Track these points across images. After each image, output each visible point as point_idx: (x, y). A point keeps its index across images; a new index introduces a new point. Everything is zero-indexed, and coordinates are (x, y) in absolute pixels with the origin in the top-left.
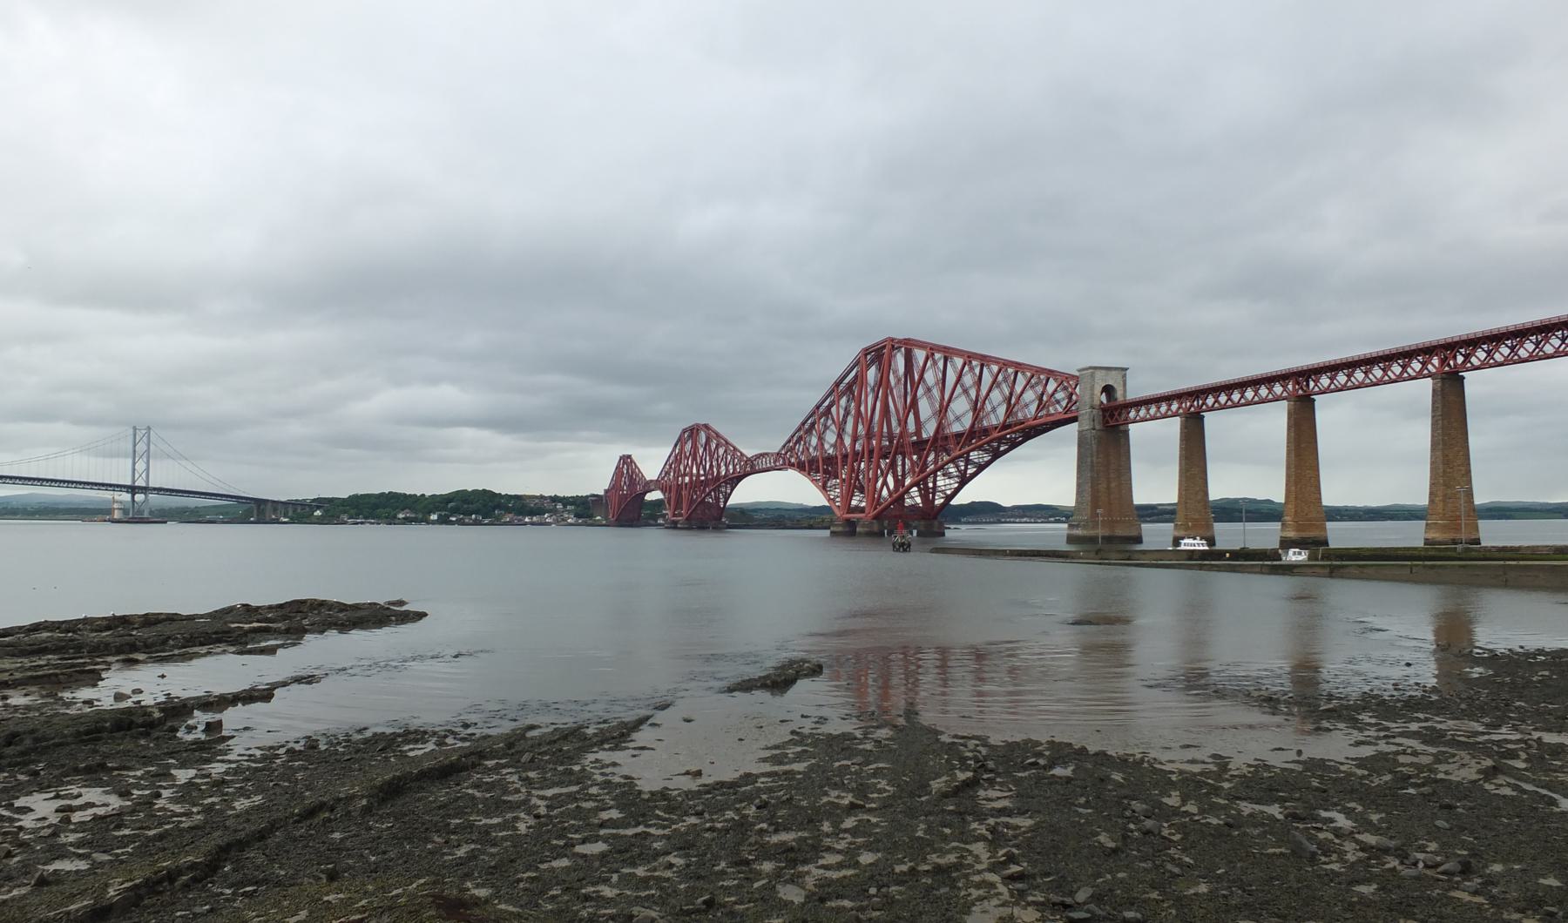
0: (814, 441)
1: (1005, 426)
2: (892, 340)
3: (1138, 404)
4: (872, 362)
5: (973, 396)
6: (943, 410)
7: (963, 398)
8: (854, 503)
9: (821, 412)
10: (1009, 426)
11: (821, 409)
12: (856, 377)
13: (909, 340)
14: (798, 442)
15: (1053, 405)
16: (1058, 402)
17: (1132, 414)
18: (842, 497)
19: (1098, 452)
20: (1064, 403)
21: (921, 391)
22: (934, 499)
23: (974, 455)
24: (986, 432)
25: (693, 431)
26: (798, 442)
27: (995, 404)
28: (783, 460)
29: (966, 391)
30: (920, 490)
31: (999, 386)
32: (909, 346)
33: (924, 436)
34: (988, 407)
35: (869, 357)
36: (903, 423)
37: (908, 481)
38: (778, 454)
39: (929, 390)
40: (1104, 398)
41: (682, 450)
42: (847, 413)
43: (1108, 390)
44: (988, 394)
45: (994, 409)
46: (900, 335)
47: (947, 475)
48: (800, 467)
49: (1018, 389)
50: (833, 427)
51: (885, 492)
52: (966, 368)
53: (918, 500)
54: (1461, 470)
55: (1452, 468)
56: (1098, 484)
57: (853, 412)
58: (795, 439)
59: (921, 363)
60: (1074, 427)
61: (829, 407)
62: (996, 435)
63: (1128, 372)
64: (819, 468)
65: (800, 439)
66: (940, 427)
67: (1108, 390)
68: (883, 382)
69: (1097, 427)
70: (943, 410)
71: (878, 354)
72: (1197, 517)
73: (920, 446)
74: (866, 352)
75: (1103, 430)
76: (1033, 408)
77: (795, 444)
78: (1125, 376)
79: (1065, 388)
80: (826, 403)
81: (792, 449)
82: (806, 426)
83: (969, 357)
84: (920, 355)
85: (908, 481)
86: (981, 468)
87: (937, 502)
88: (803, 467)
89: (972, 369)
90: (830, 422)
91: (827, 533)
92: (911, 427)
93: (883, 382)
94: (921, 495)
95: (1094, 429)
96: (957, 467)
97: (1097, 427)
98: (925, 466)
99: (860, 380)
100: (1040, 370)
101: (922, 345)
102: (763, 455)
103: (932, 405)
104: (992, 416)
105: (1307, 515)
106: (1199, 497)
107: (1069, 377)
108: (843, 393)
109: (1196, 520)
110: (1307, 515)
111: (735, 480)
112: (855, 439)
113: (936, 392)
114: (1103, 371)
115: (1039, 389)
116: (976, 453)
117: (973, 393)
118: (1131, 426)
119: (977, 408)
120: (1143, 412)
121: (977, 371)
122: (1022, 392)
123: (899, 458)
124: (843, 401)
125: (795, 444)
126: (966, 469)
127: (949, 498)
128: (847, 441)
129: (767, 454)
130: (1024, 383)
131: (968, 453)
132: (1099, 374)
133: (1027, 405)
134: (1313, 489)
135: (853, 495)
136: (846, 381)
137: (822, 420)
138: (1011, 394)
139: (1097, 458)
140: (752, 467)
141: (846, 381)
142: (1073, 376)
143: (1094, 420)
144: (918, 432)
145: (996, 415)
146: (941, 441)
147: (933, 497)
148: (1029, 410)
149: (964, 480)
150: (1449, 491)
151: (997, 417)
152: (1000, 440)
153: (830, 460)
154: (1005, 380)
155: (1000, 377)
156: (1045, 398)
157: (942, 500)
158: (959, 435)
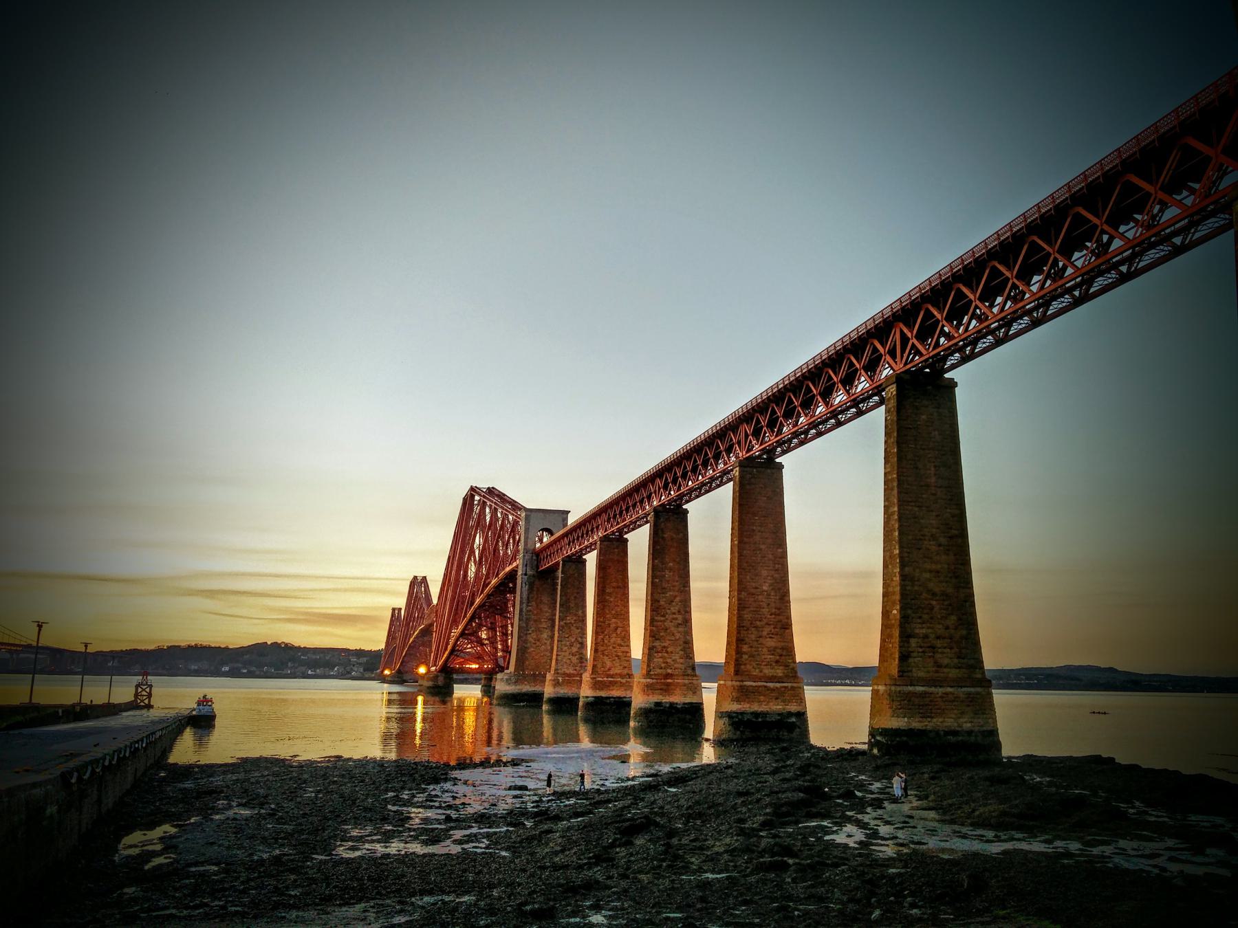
19: (528, 598)
54: (676, 619)
55: (662, 616)
56: (526, 634)
69: (529, 572)
72: (571, 671)
75: (534, 576)
78: (566, 519)
95: (526, 574)
97: (529, 572)
105: (609, 669)
106: (574, 649)
109: (569, 675)
110: (609, 669)
134: (619, 641)
139: (528, 606)
143: (526, 566)
150: (657, 644)
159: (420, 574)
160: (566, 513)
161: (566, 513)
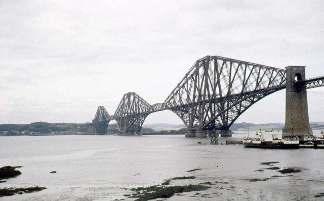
0: (178, 98)
2: (208, 56)
3: (310, 81)
4: (201, 65)
5: (243, 79)
8: (195, 123)
9: (180, 87)
10: (258, 91)
11: (181, 85)
12: (195, 72)
13: (216, 56)
14: (171, 98)
15: (275, 82)
16: (277, 81)
17: (308, 85)
18: (189, 120)
20: (280, 81)
21: (221, 77)
22: (227, 121)
23: (244, 103)
24: (248, 93)
25: (129, 95)
26: (171, 98)
27: (252, 82)
28: (165, 107)
29: (239, 77)
30: (221, 117)
31: (253, 74)
32: (216, 58)
33: (223, 96)
35: (200, 63)
36: (214, 91)
37: (216, 114)
38: (163, 104)
40: (296, 79)
41: (124, 102)
42: (191, 87)
43: (299, 76)
44: (248, 78)
45: (251, 84)
46: (212, 54)
47: (232, 111)
48: (173, 109)
49: (261, 75)
50: (186, 92)
51: (207, 119)
52: (240, 67)
53: (221, 122)
57: (193, 86)
58: (170, 97)
60: (284, 90)
61: (184, 84)
62: (252, 94)
63: (306, 68)
64: (180, 109)
65: (173, 97)
66: (229, 92)
67: (299, 76)
68: (206, 74)
71: (205, 62)
73: (222, 100)
74: (198, 62)
76: (267, 83)
77: (170, 100)
78: (304, 70)
79: (280, 75)
80: (183, 83)
81: (169, 101)
82: (175, 92)
83: (240, 63)
84: (220, 62)
85: (216, 114)
86: (246, 108)
87: (228, 122)
88: (174, 109)
89: (242, 68)
90: (184, 90)
91: (184, 136)
92: (217, 92)
93: (206, 74)
94: (222, 120)
98: (223, 108)
99: (197, 72)
100: (271, 68)
101: (221, 58)
102: (157, 104)
103: (226, 83)
104: (250, 87)
107: (280, 71)
108: (190, 78)
111: (146, 115)
112: (194, 97)
113: (227, 78)
114: (296, 68)
115: (270, 75)
116: (244, 102)
118: (307, 90)
119: (244, 85)
120: (312, 84)
121: (244, 68)
122: (263, 77)
123: (213, 104)
124: (189, 82)
125: (170, 100)
126: (240, 108)
127: (233, 121)
128: (191, 98)
129: (159, 104)
130: (263, 73)
131: (241, 102)
132: (294, 69)
133: (265, 82)
135: (194, 120)
136: (191, 73)
137: (181, 90)
138: (258, 78)
140: (153, 109)
141: (191, 73)
142: (283, 70)
144: (220, 94)
145: (252, 87)
146: (229, 97)
147: (227, 120)
148: (265, 84)
149: (240, 113)
151: (252, 87)
152: (254, 96)
153: (184, 106)
154: (256, 71)
155: (253, 71)
156: (272, 79)
157: (231, 122)
159: (132, 92)
160: (304, 68)
161: (304, 68)
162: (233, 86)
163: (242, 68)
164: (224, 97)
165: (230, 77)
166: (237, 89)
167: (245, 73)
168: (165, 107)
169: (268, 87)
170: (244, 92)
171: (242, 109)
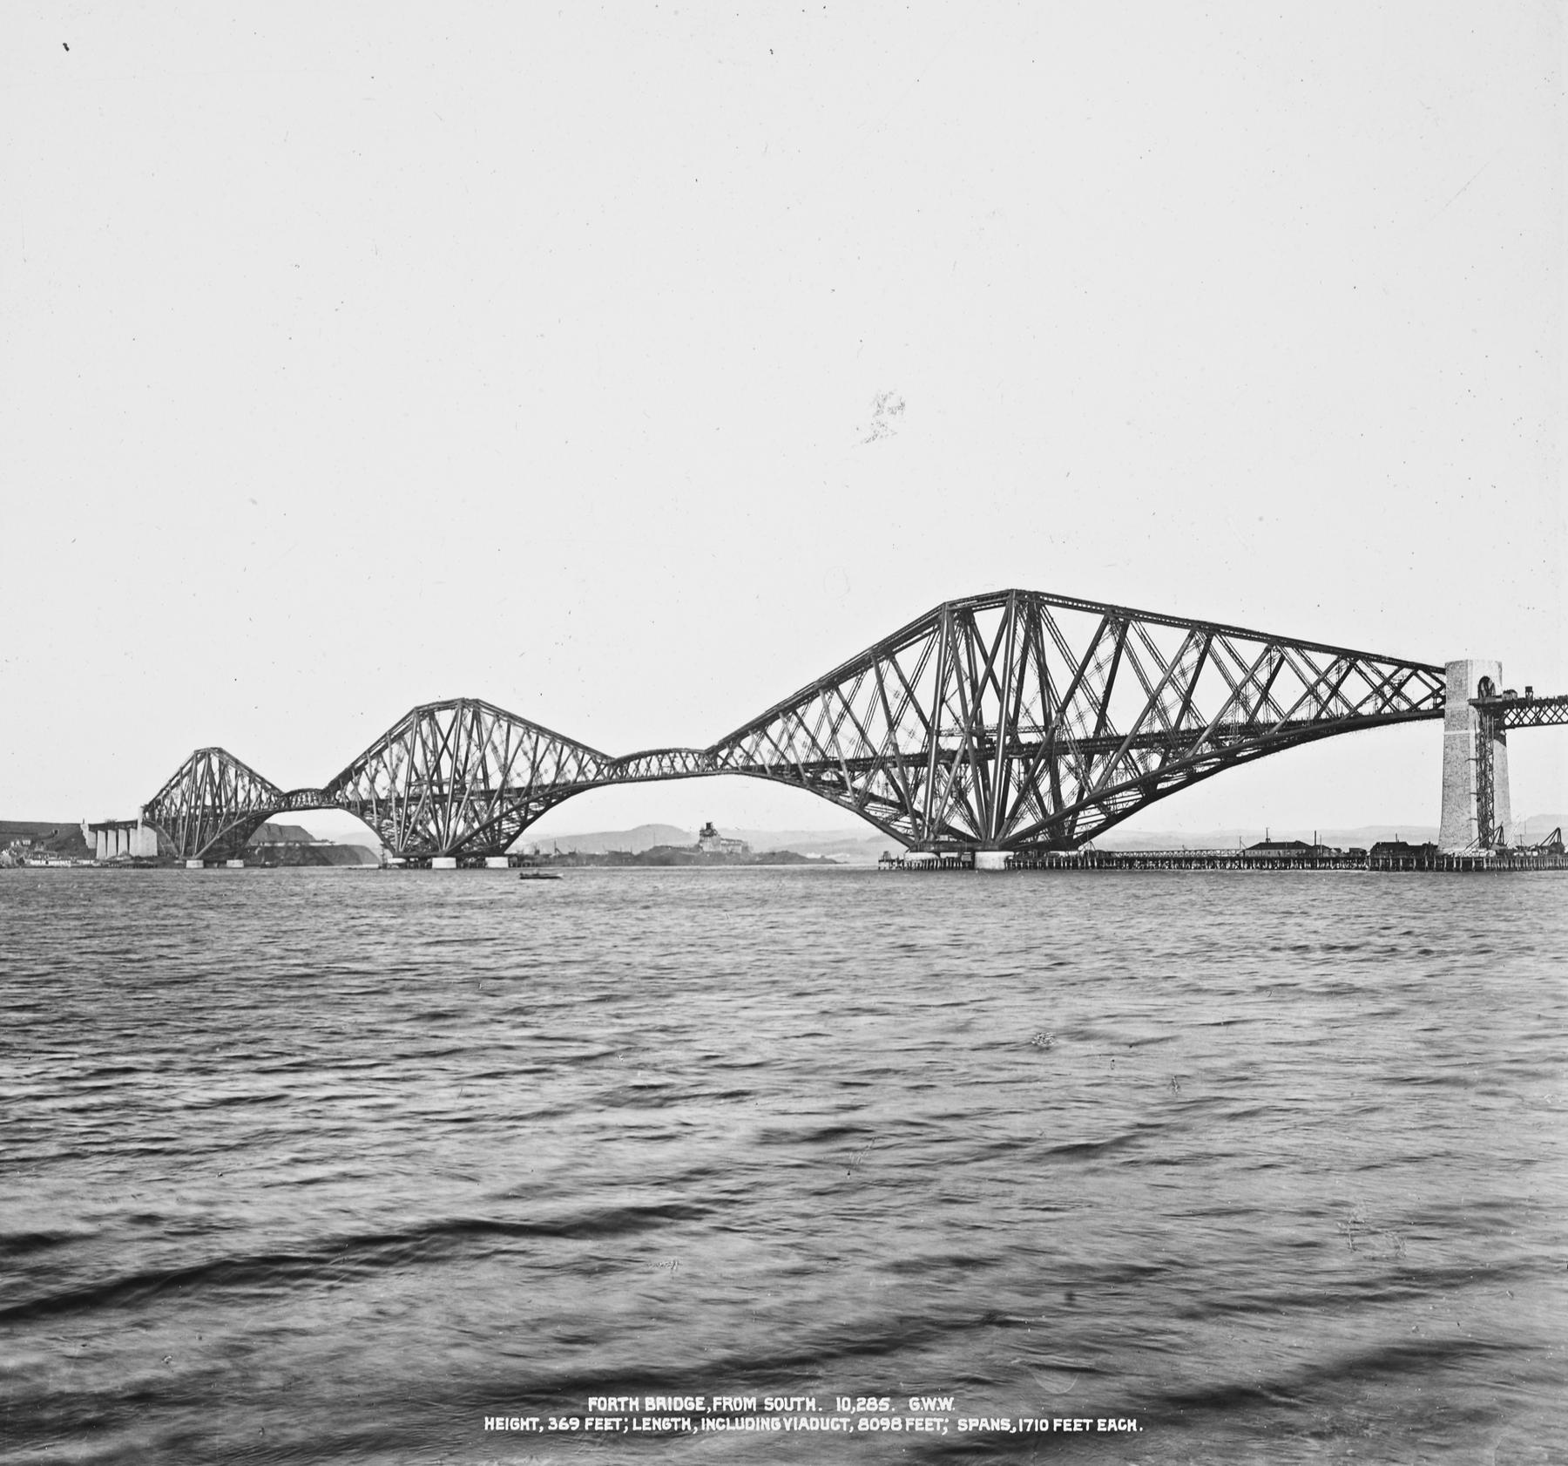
1: (554, 785)
6: (505, 769)
7: (524, 758)
21: (489, 748)
24: (542, 787)
28: (327, 797)
29: (525, 754)
33: (492, 786)
34: (542, 769)
39: (495, 749)
45: (546, 771)
47: (512, 820)
59: (490, 726)
70: (505, 769)
73: (488, 795)
84: (488, 719)
86: (538, 815)
89: (530, 737)
96: (519, 814)
101: (490, 707)
117: (531, 755)
119: (535, 768)
131: (527, 803)
145: (547, 779)
146: (505, 792)
149: (525, 824)
158: (519, 790)
162: (513, 773)
163: (530, 737)
164: (494, 791)
165: (507, 751)
166: (521, 778)
167: (535, 749)
168: (327, 797)
169: (575, 781)
170: (534, 784)
171: (529, 817)
